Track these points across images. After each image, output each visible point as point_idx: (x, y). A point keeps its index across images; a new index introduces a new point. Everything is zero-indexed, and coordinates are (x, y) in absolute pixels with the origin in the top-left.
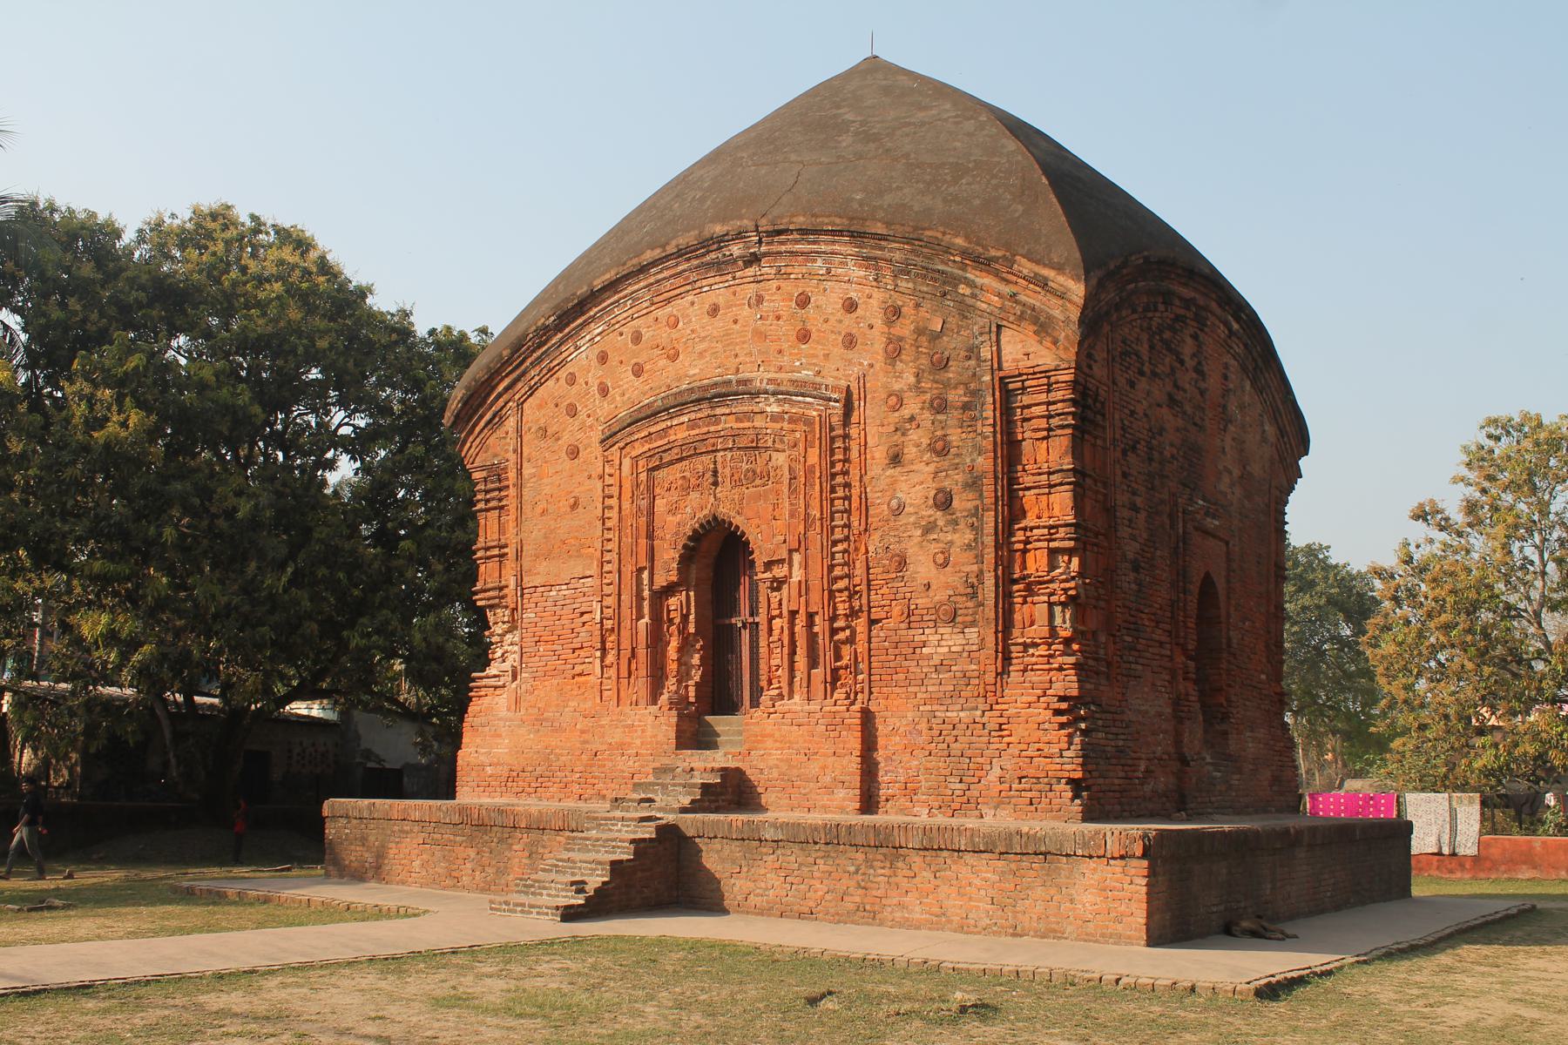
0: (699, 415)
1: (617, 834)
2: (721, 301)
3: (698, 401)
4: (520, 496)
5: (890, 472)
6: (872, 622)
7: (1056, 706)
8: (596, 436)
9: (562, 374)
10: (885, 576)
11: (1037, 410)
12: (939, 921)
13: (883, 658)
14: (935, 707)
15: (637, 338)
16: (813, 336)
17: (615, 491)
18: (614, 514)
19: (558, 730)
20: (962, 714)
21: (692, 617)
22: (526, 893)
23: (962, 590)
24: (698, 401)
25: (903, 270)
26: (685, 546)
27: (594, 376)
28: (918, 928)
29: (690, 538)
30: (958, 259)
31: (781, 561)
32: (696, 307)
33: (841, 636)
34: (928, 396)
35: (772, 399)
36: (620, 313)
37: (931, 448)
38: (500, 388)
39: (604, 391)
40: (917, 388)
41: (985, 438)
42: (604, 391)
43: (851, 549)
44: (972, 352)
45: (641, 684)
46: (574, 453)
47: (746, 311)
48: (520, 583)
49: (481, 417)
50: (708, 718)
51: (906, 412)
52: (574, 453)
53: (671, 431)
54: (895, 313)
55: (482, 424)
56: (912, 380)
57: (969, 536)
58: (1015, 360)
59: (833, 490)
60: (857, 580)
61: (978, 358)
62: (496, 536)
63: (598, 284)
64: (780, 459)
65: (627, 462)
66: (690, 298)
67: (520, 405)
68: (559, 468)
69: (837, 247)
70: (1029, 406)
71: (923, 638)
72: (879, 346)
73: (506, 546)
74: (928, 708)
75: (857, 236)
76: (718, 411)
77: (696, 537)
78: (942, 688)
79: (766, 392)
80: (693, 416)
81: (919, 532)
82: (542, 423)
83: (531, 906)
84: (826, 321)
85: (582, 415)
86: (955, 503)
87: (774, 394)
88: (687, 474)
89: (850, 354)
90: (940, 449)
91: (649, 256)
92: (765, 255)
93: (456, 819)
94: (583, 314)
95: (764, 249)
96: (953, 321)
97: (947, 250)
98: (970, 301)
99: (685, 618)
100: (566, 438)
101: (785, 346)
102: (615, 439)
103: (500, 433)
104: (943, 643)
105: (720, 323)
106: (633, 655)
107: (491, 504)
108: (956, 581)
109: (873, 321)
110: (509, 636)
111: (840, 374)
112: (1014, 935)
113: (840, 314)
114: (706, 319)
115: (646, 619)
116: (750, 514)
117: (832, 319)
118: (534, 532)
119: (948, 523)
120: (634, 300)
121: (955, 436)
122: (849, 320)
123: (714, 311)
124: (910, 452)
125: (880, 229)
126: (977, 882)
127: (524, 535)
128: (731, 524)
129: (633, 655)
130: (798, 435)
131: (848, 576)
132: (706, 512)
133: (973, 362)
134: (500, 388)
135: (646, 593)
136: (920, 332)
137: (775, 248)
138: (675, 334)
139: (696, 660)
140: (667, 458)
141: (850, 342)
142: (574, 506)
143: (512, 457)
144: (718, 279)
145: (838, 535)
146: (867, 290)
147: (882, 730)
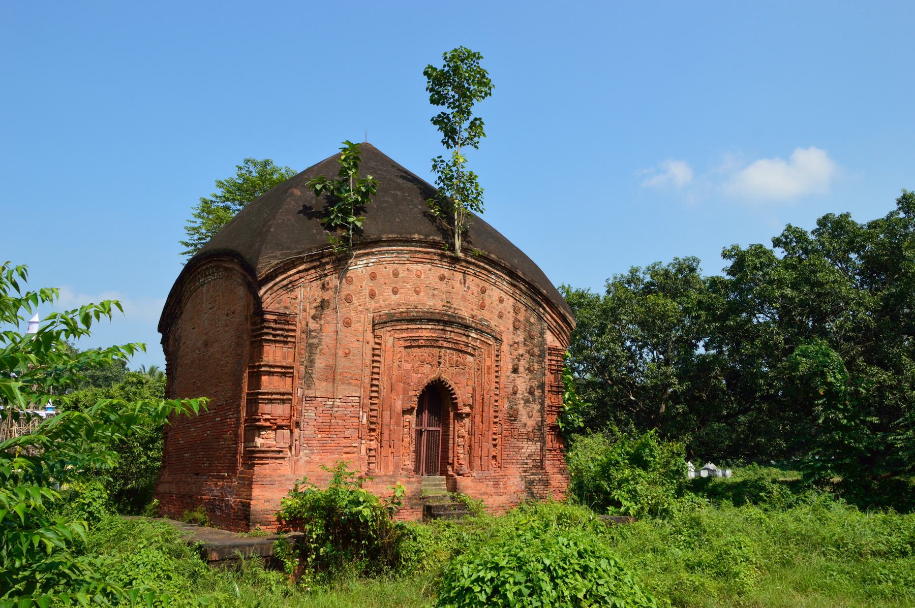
2: (446, 274)
3: (438, 321)
11: (553, 362)
15: (396, 274)
26: (423, 391)
27: (367, 285)
36: (387, 257)
37: (528, 369)
39: (372, 295)
42: (372, 295)
44: (542, 334)
52: (347, 324)
54: (516, 311)
55: (280, 285)
63: (384, 237)
66: (429, 266)
72: (511, 321)
75: (511, 274)
87: (476, 330)
89: (501, 321)
90: (530, 370)
91: (416, 236)
94: (365, 248)
97: (541, 294)
101: (475, 307)
105: (443, 286)
107: (278, 338)
108: (534, 422)
114: (437, 280)
122: (501, 306)
123: (442, 278)
124: (521, 369)
125: (520, 274)
136: (527, 320)
141: (500, 316)
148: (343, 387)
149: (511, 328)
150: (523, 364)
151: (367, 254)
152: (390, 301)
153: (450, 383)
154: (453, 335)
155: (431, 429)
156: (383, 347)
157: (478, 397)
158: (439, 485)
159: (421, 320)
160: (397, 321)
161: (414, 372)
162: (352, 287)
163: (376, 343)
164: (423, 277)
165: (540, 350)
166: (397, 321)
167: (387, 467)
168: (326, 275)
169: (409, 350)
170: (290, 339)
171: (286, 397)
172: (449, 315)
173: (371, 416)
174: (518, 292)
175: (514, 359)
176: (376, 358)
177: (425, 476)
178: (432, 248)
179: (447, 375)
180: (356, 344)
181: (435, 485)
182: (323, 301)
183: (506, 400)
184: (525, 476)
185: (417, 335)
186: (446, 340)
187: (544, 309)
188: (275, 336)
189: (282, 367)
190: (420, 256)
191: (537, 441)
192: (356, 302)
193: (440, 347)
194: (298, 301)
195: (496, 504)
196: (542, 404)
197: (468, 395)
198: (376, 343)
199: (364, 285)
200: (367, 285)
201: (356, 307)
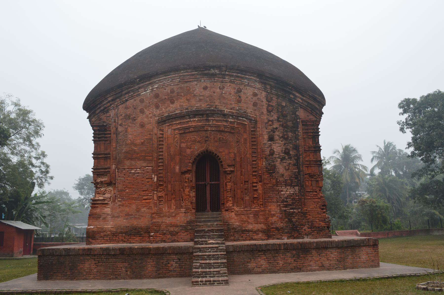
1: (210, 254)
2: (208, 85)
3: (202, 115)
5: (269, 142)
7: (322, 207)
9: (138, 99)
11: (310, 131)
12: (322, 268)
13: (269, 195)
16: (243, 101)
20: (295, 210)
22: (199, 277)
26: (195, 159)
28: (315, 271)
29: (197, 156)
34: (281, 123)
35: (231, 117)
44: (294, 113)
46: (142, 125)
47: (218, 90)
51: (275, 126)
53: (190, 122)
56: (276, 118)
57: (295, 161)
61: (295, 114)
66: (196, 83)
69: (252, 77)
70: (307, 129)
71: (282, 189)
72: (265, 107)
74: (284, 209)
76: (210, 118)
79: (230, 115)
81: (280, 160)
83: (214, 281)
84: (247, 97)
86: (291, 153)
87: (232, 116)
89: (255, 108)
90: (284, 138)
92: (227, 75)
93: (118, 252)
94: (150, 80)
95: (227, 73)
98: (294, 100)
104: (287, 191)
105: (207, 93)
111: (253, 113)
112: (344, 269)
114: (202, 90)
116: (221, 151)
117: (250, 97)
120: (173, 79)
121: (290, 134)
122: (255, 98)
123: (205, 88)
124: (276, 137)
126: (333, 256)
128: (213, 153)
132: (204, 149)
133: (294, 116)
136: (279, 104)
137: (230, 73)
141: (255, 104)
144: (208, 79)
149: (265, 111)
151: (150, 84)
153: (215, 153)
155: (213, 183)
156: (164, 137)
157: (238, 159)
158: (217, 217)
160: (172, 119)
161: (188, 148)
162: (144, 104)
166: (172, 119)
167: (170, 207)
168: (127, 100)
169: (184, 135)
171: (106, 170)
172: (211, 110)
173: (160, 177)
174: (268, 87)
175: (269, 132)
176: (161, 143)
177: (210, 213)
178: (196, 71)
179: (212, 148)
182: (126, 115)
183: (264, 160)
184: (285, 211)
185: (188, 125)
188: (99, 138)
190: (188, 77)
191: (295, 186)
192: (147, 112)
193: (207, 130)
194: (111, 117)
195: (255, 229)
196: (298, 160)
198: (161, 134)
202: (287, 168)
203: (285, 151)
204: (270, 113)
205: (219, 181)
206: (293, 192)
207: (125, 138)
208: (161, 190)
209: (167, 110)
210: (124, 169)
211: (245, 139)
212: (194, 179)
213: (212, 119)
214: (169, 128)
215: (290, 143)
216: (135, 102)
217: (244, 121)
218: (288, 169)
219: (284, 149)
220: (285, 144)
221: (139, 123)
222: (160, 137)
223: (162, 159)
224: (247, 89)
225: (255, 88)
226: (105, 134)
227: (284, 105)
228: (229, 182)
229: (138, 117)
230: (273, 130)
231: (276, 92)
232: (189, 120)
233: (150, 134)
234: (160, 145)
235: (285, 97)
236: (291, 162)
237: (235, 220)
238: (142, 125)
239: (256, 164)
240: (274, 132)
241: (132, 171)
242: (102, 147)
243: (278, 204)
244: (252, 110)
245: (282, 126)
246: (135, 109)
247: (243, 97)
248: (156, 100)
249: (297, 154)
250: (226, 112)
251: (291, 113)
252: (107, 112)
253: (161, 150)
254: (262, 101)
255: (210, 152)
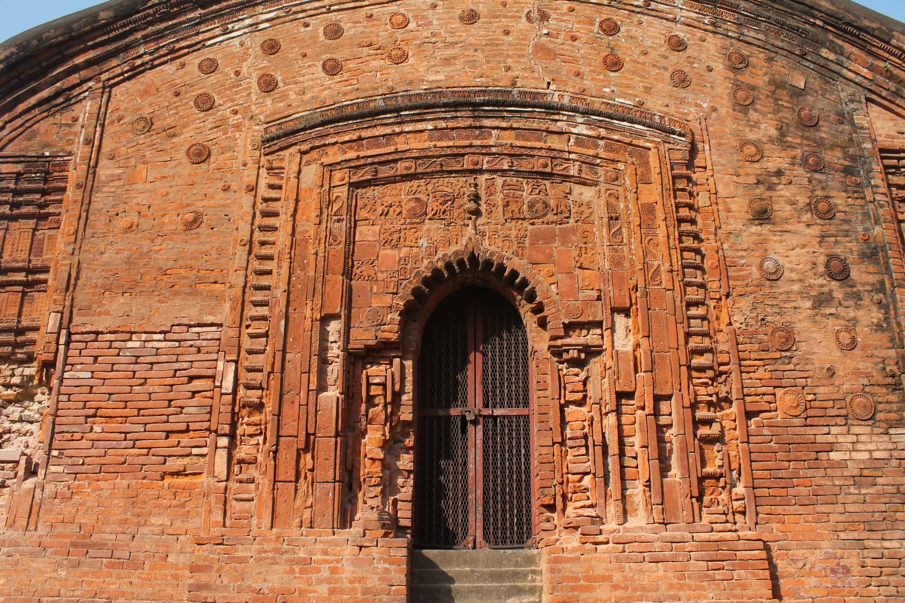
0: (451, 124)
3: (455, 106)
4: (87, 204)
5: (754, 229)
6: (749, 415)
8: (258, 131)
9: (193, 61)
10: (763, 355)
14: (865, 535)
15: (335, 32)
17: (284, 208)
18: (282, 238)
19: (133, 564)
21: (406, 398)
23: (881, 380)
24: (455, 106)
25: (755, 19)
26: (416, 292)
29: (426, 281)
30: (818, 22)
31: (599, 325)
32: (439, 10)
33: (703, 431)
34: (799, 152)
35: (580, 119)
37: (811, 207)
38: (80, 60)
39: (268, 85)
40: (781, 140)
41: (882, 206)
43: (713, 313)
45: (327, 494)
46: (200, 155)
47: (523, 24)
48: (66, 324)
49: (34, 92)
50: (429, 553)
51: (771, 165)
53: (401, 139)
54: (738, 64)
55: (33, 100)
56: (773, 132)
57: (877, 315)
58: (888, 136)
59: (681, 241)
60: (723, 358)
61: (852, 123)
62: (25, 256)
64: (588, 193)
65: (311, 174)
67: (108, 87)
68: (168, 171)
71: (830, 439)
72: (723, 89)
73: (46, 270)
74: (856, 535)
76: (487, 123)
77: (434, 279)
78: (866, 507)
79: (575, 110)
80: (444, 125)
81: (808, 304)
82: (146, 112)
85: (224, 110)
86: (854, 274)
87: (585, 113)
88: (425, 198)
89: (682, 93)
96: (816, 83)
99: (397, 396)
100: (187, 137)
101: (585, 69)
102: (292, 140)
103: (64, 118)
105: (476, 33)
106: (308, 447)
107: (24, 210)
109: (713, 65)
110: (14, 411)
111: (672, 110)
113: (663, 50)
114: (457, 24)
115: (333, 393)
117: (653, 54)
118: (106, 254)
119: (848, 296)
121: (840, 200)
124: (782, 209)
127: (83, 256)
128: (502, 268)
129: (308, 447)
130: (621, 166)
131: (711, 351)
132: (454, 248)
134: (80, 60)
135: (335, 351)
136: (778, 84)
138: (400, 35)
139: (406, 461)
140: (385, 172)
141: (681, 80)
142: (194, 223)
143: (80, 150)
145: (693, 294)
146: (699, 33)
147: (781, 564)
148: (178, 301)
150: (787, 197)
152: (310, 88)
154: (508, 138)
155: (498, 412)
158: (515, 574)
159: (397, 110)
160: (323, 124)
162: (213, 78)
163: (272, 187)
164: (412, 25)
165: (847, 156)
166: (323, 124)
169: (370, 192)
170: (51, 210)
174: (729, 16)
175: (747, 186)
177: (485, 552)
179: (496, 240)
180: (221, 197)
181: (499, 577)
185: (392, 149)
186: (485, 150)
187: (833, 49)
189: (29, 271)
194: (77, 128)
197: (581, 296)
198: (272, 187)
199: (244, 70)
200: (254, 67)
201: (224, 120)
202: (845, 338)
203: (827, 266)
204: (746, 114)
205: (526, 404)
206: (884, 455)
207: (121, 208)
208: (251, 430)
209: (307, 97)
210: (97, 333)
211: (649, 209)
212: (409, 387)
213: (497, 123)
214: (308, 163)
215: (847, 234)
216: (181, 72)
217: (642, 135)
218: (853, 345)
219: (822, 259)
220: (823, 237)
221: (185, 148)
222: (266, 200)
223: (267, 288)
224: (640, 23)
225: (674, 20)
226: (44, 193)
227: (802, 86)
228: (581, 403)
229: (186, 125)
230: (769, 181)
231: (761, 36)
232: (397, 129)
233: (226, 189)
234: (264, 229)
235: (803, 56)
236: (860, 313)
237: (616, 587)
238: (199, 155)
239: (703, 318)
240: (771, 188)
241: (130, 344)
242: (26, 243)
243: (819, 508)
244: (666, 102)
245: (805, 163)
246: (177, 94)
247: (628, 53)
248: (265, 63)
249: (882, 283)
250: (556, 99)
251: (833, 117)
252: (68, 104)
253: (264, 251)
254: (710, 69)
255: (488, 263)
